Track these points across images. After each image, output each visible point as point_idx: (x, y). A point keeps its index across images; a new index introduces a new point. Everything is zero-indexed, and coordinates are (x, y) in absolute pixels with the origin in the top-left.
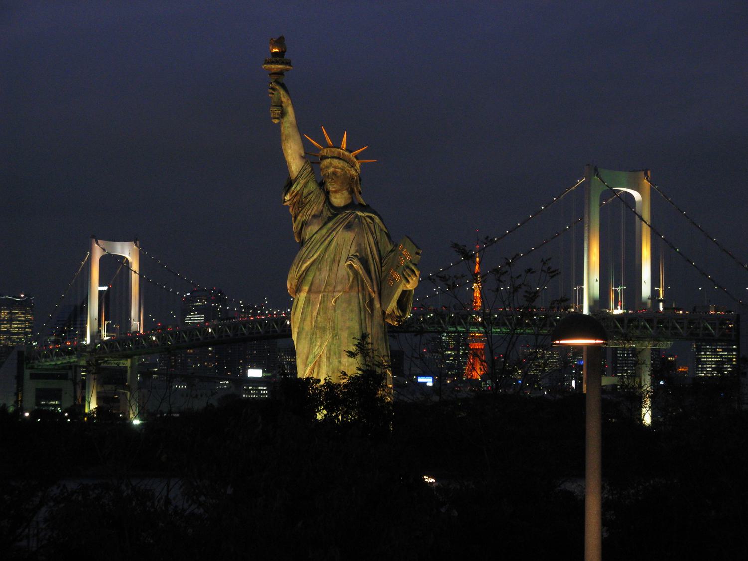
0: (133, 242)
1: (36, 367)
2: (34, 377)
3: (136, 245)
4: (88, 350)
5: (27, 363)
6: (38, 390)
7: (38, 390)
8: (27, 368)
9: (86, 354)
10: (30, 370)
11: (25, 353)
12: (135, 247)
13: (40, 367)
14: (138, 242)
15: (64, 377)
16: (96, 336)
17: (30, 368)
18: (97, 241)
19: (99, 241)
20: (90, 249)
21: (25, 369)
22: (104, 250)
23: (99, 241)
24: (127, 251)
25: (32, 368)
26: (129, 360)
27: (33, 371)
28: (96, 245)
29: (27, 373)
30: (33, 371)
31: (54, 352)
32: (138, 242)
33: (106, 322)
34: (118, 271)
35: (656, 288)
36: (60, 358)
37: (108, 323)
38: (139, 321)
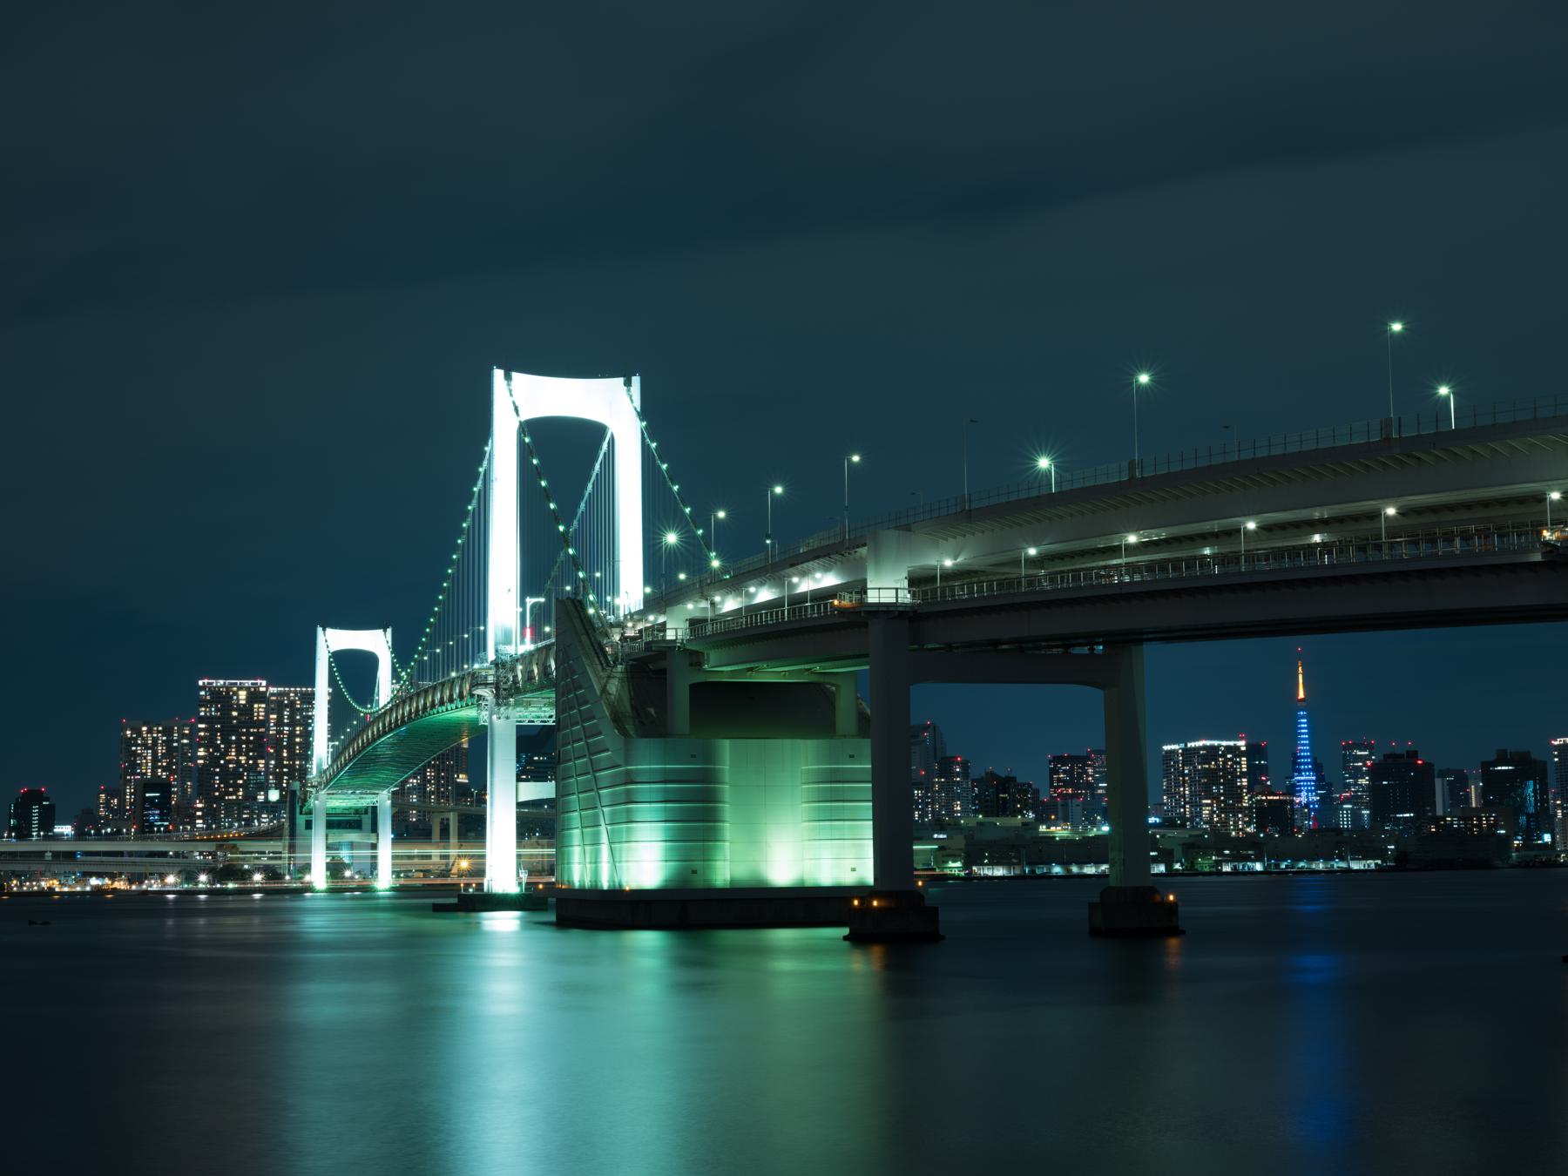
5: (301, 808)
8: (301, 813)
11: (298, 793)
14: (389, 631)
16: (319, 766)
17: (306, 814)
18: (324, 630)
23: (329, 630)
24: (376, 642)
28: (323, 635)
32: (389, 631)
37: (333, 746)
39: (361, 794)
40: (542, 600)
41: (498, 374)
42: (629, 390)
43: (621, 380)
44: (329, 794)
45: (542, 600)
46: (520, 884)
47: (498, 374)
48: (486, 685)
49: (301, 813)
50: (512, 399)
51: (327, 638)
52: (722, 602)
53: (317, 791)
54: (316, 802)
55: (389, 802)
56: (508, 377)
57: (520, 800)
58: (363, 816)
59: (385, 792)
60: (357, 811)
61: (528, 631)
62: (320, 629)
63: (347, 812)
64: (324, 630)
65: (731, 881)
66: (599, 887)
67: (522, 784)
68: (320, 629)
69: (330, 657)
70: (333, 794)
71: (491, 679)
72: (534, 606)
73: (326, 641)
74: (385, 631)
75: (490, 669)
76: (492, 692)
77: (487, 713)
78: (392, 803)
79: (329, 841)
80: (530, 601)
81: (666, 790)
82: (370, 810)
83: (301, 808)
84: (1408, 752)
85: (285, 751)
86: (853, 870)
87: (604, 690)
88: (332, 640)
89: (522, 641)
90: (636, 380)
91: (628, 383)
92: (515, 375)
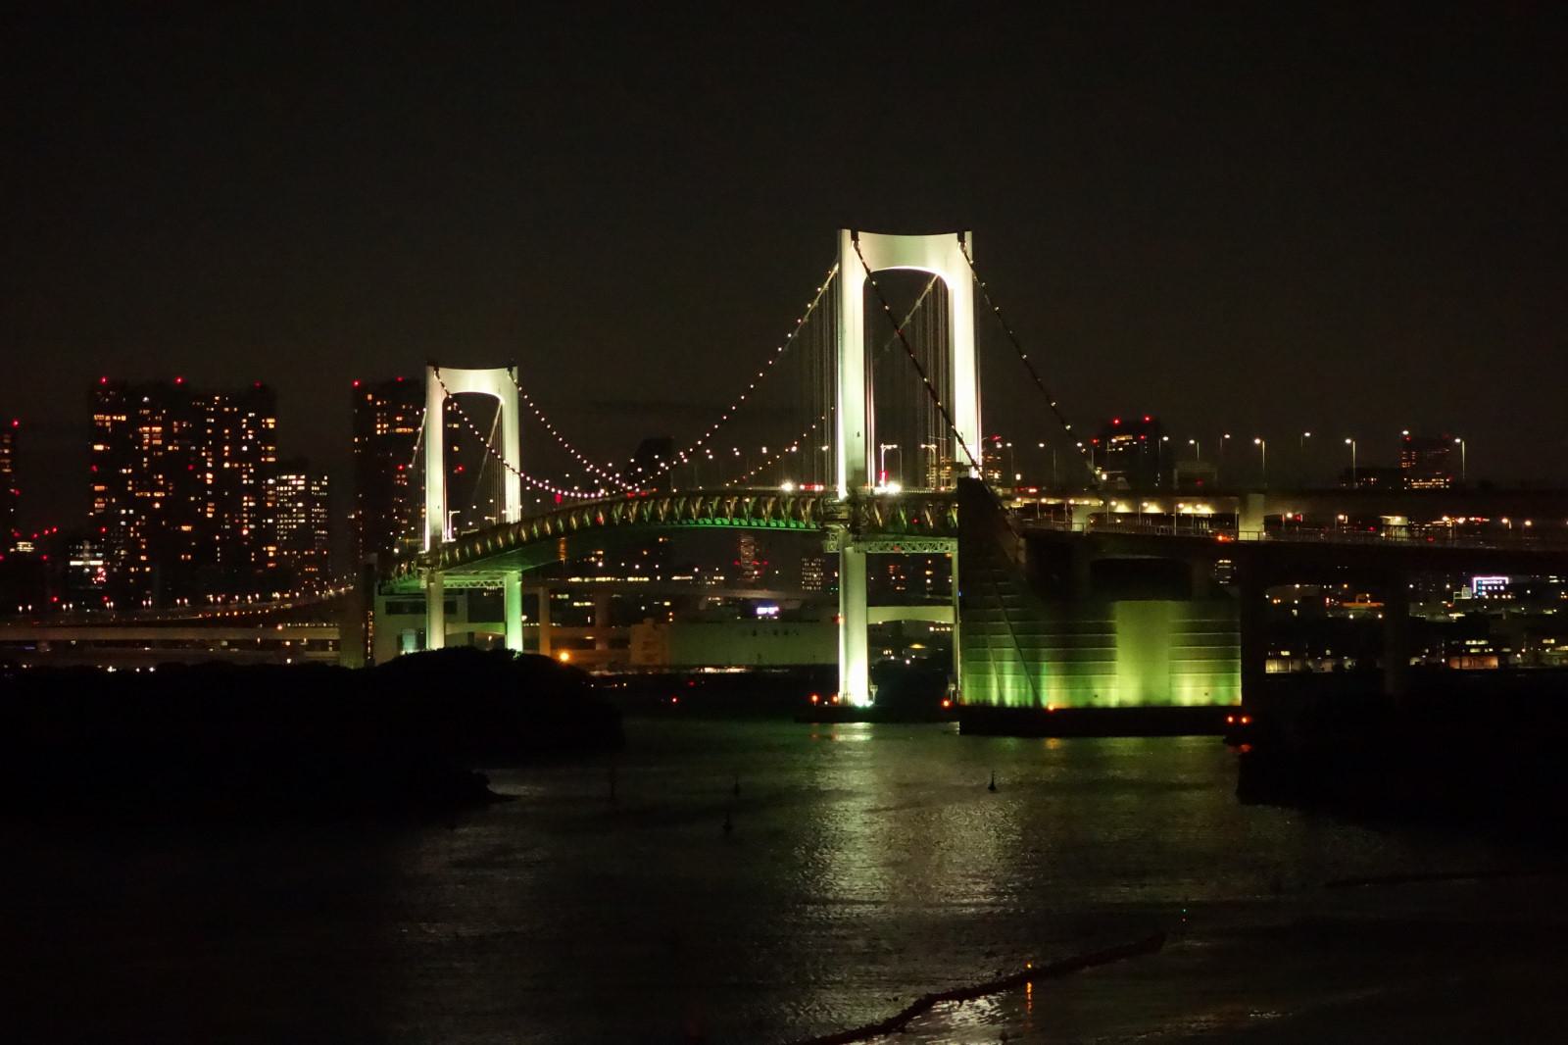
0: (506, 369)
1: (397, 591)
3: (511, 375)
8: (380, 594)
10: (386, 597)
11: (376, 568)
12: (509, 378)
14: (515, 369)
16: (436, 539)
17: (386, 594)
23: (442, 371)
27: (390, 599)
28: (435, 377)
29: (381, 601)
30: (390, 599)
33: (451, 513)
37: (453, 515)
39: (485, 573)
41: (847, 233)
42: (963, 246)
43: (955, 235)
44: (446, 574)
46: (871, 698)
47: (847, 233)
48: (842, 521)
49: (380, 594)
52: (1116, 507)
53: (432, 572)
54: (432, 584)
55: (519, 584)
56: (855, 238)
57: (871, 622)
58: (457, 596)
59: (514, 572)
61: (883, 474)
64: (437, 370)
65: (1120, 702)
66: (962, 703)
67: (870, 608)
69: (447, 402)
71: (844, 515)
72: (887, 451)
73: (443, 385)
74: (510, 370)
75: (841, 504)
76: (846, 526)
77: (835, 542)
78: (522, 586)
79: (448, 633)
80: (884, 448)
83: (380, 587)
85: (209, 482)
86: (1206, 694)
87: (1017, 560)
90: (968, 235)
91: (961, 239)
92: (861, 235)
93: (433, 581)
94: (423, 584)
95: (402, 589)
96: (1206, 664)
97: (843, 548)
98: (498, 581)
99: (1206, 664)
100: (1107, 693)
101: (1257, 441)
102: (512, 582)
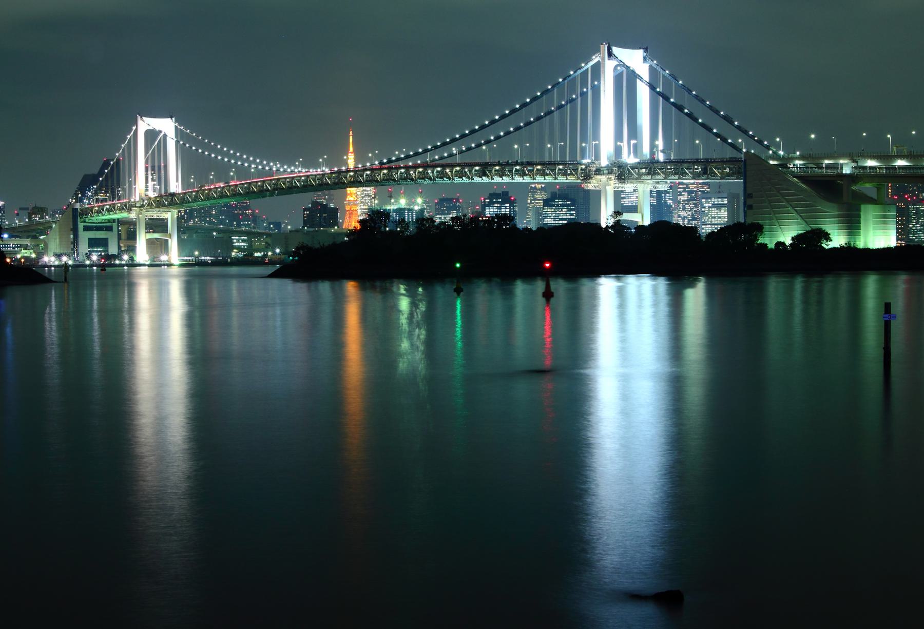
0: (170, 119)
1: (87, 221)
2: (87, 229)
4: (138, 205)
6: (90, 240)
7: (90, 240)
9: (136, 209)
13: (91, 221)
14: (173, 119)
15: (110, 229)
18: (141, 118)
19: (143, 118)
20: (137, 124)
21: (79, 222)
22: (149, 125)
24: (167, 126)
25: (84, 222)
26: (169, 213)
29: (81, 226)
31: (105, 209)
32: (173, 119)
33: (153, 183)
34: (156, 143)
35: (619, 143)
36: (111, 213)
38: (177, 181)
40: (635, 142)
45: (635, 142)
50: (619, 59)
51: (145, 124)
54: (140, 216)
55: (176, 216)
58: (113, 223)
60: (109, 221)
61: (632, 154)
62: (139, 118)
63: (103, 221)
68: (139, 118)
70: (148, 211)
74: (172, 119)
80: (633, 142)
81: (876, 221)
82: (116, 220)
84: (503, 192)
88: (145, 124)
89: (629, 156)
93: (141, 214)
94: (133, 215)
95: (89, 220)
96: (846, 232)
97: (605, 188)
98: (162, 215)
99: (843, 232)
100: (860, 244)
101: (889, 136)
102: (170, 216)
